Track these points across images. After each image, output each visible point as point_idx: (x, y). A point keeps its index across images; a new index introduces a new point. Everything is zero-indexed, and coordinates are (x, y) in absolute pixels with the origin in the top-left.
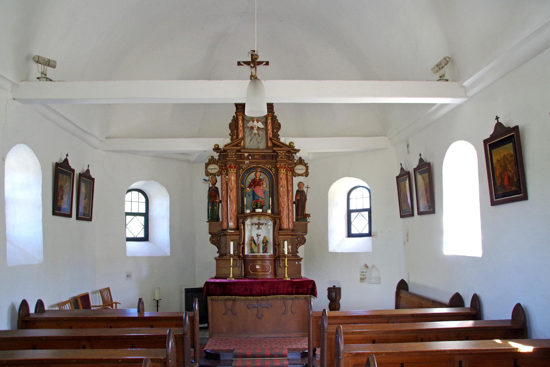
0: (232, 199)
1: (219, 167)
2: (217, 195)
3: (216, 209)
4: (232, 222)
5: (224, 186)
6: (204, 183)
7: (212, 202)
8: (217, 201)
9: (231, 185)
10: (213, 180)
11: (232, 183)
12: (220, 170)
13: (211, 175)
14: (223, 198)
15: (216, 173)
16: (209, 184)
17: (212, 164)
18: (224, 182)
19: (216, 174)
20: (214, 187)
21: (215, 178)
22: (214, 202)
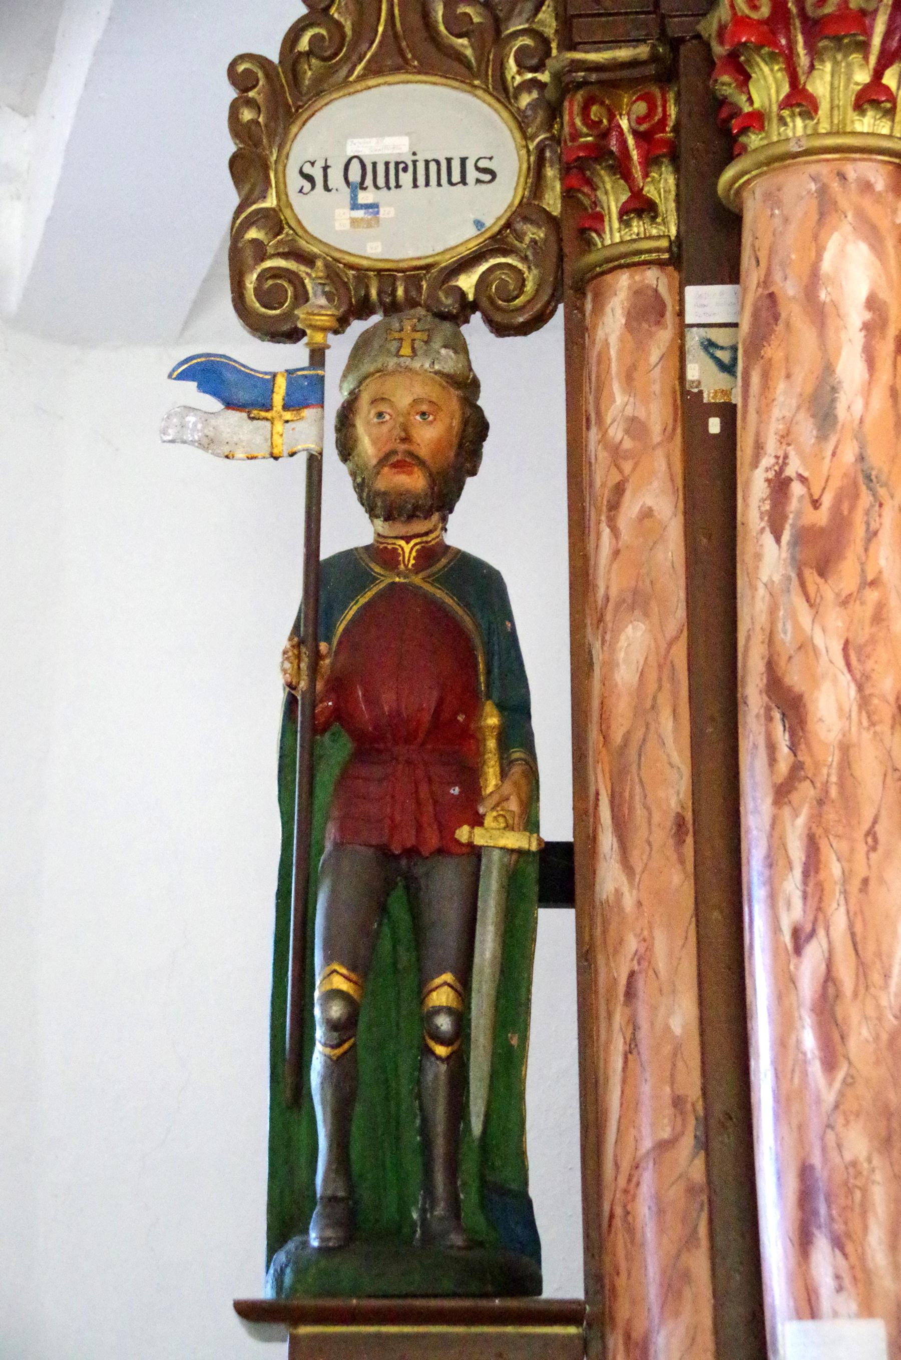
0: (845, 749)
1: (521, 122)
2: (492, 720)
3: (461, 1018)
4: (867, 1310)
5: (630, 509)
6: (208, 444)
7: (384, 853)
8: (475, 853)
9: (806, 430)
10: (403, 399)
11: (829, 369)
12: (553, 202)
13: (363, 309)
14: (619, 777)
15: (465, 264)
16: (315, 464)
17: (375, 70)
18: (636, 427)
19: (467, 282)
20: (408, 550)
21: (448, 362)
22: (412, 852)
